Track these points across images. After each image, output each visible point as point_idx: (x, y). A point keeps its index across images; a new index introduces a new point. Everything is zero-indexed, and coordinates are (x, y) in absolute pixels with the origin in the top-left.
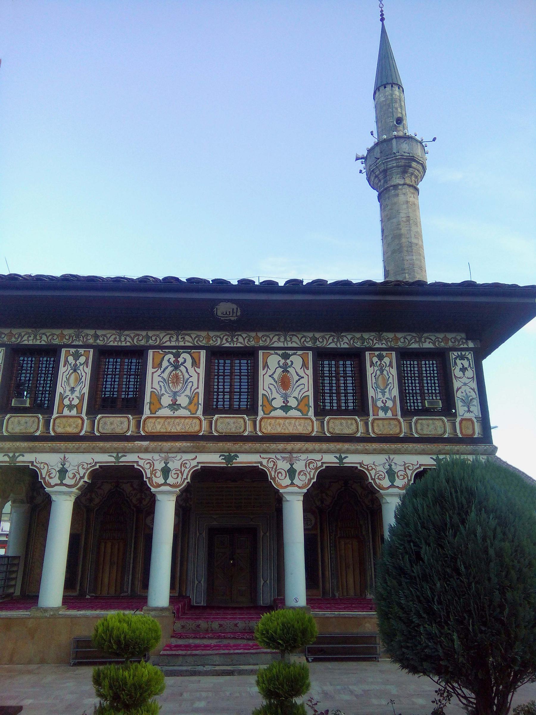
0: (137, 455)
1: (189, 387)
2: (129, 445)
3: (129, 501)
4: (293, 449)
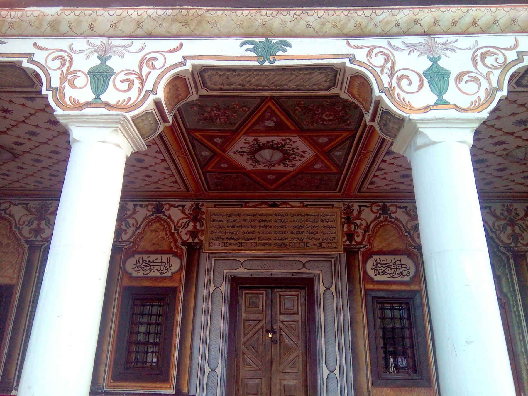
0: (30, 42)
4: (435, 23)
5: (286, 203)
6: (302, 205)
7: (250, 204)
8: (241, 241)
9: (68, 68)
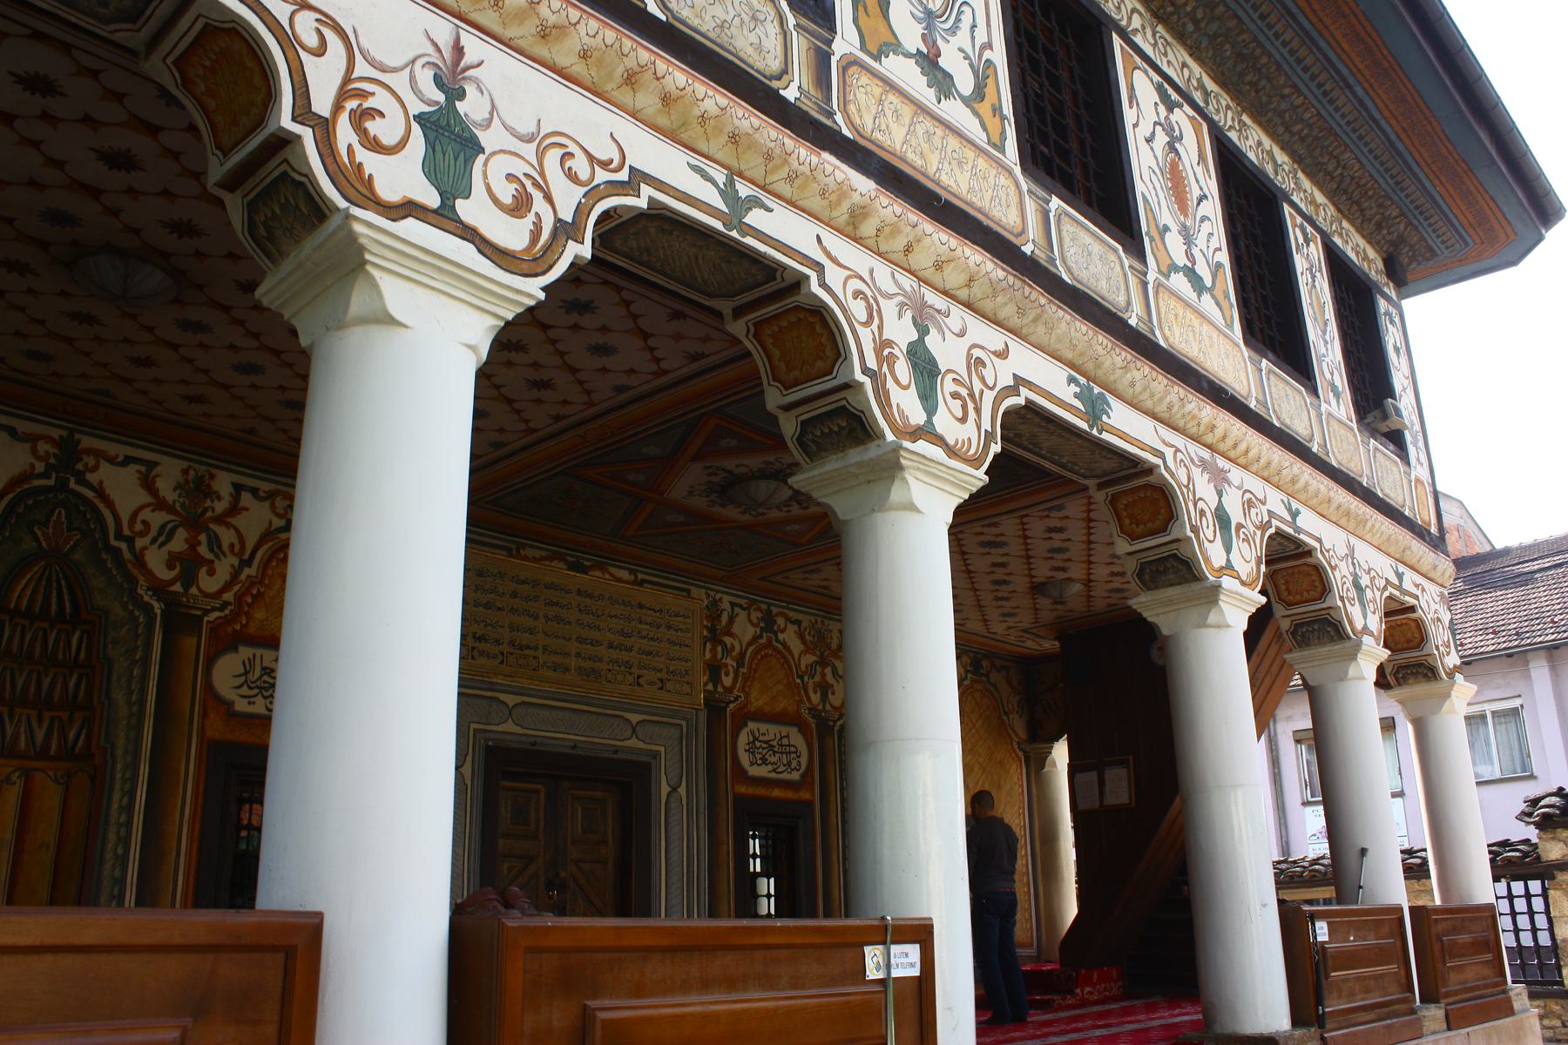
0: (814, 228)
1: (967, 19)
2: (804, 154)
3: (127, 555)
5: (603, 568)
6: (632, 578)
7: (530, 552)
8: (506, 649)
9: (880, 328)
